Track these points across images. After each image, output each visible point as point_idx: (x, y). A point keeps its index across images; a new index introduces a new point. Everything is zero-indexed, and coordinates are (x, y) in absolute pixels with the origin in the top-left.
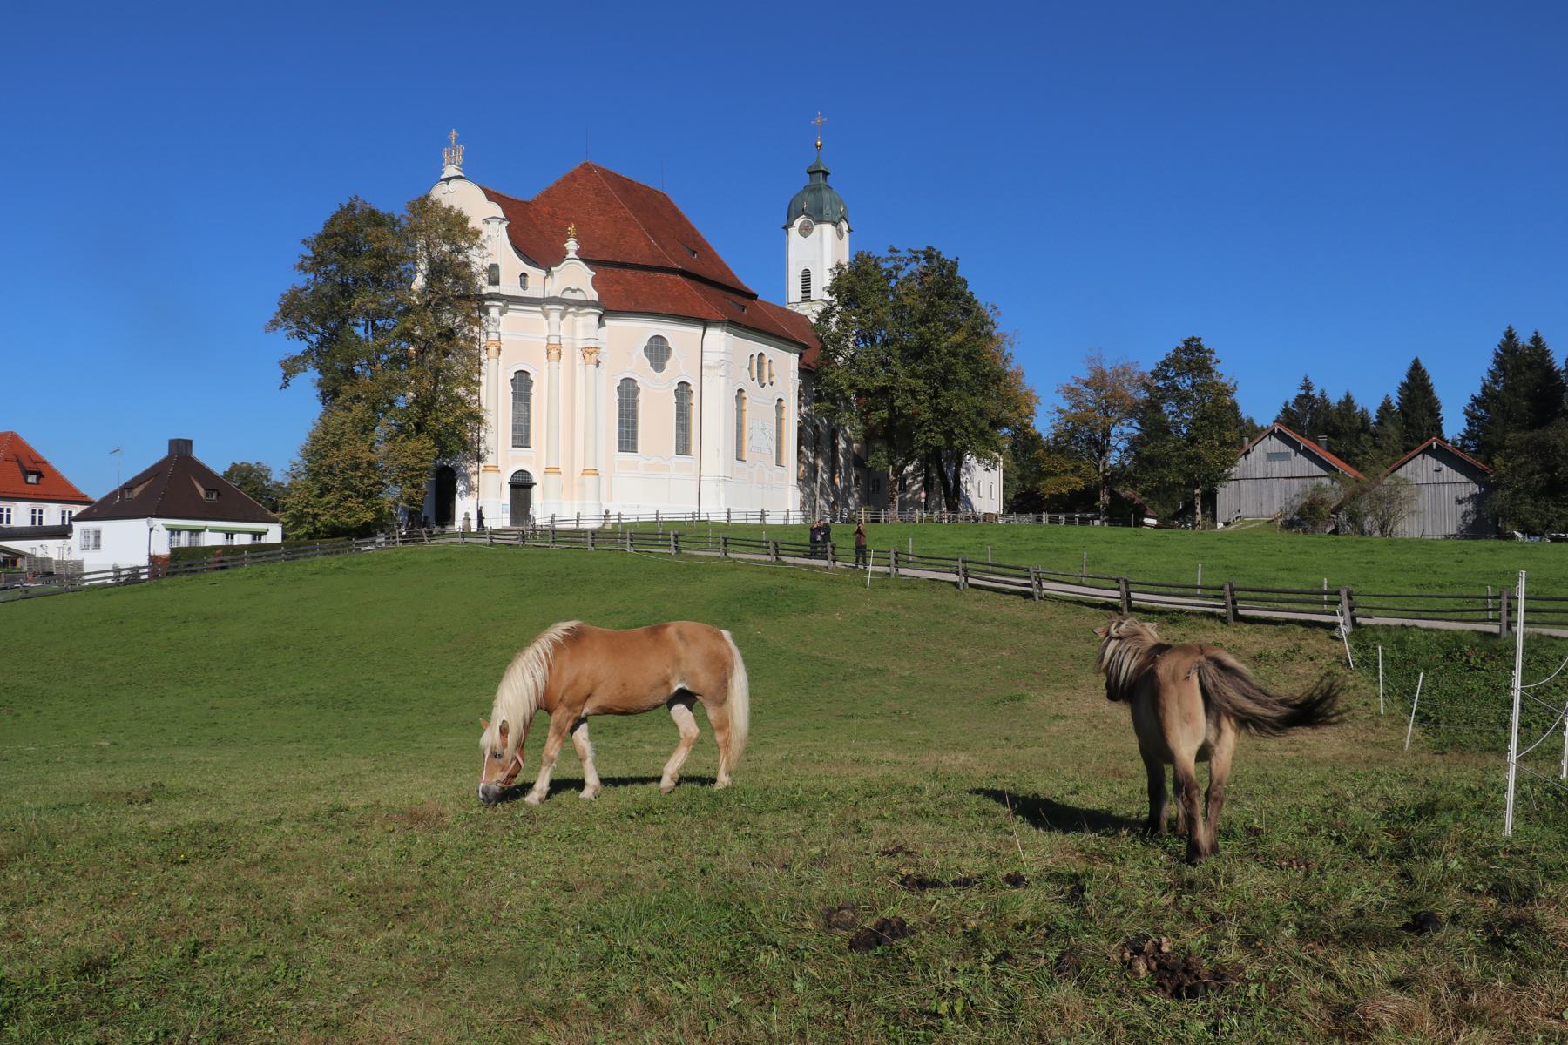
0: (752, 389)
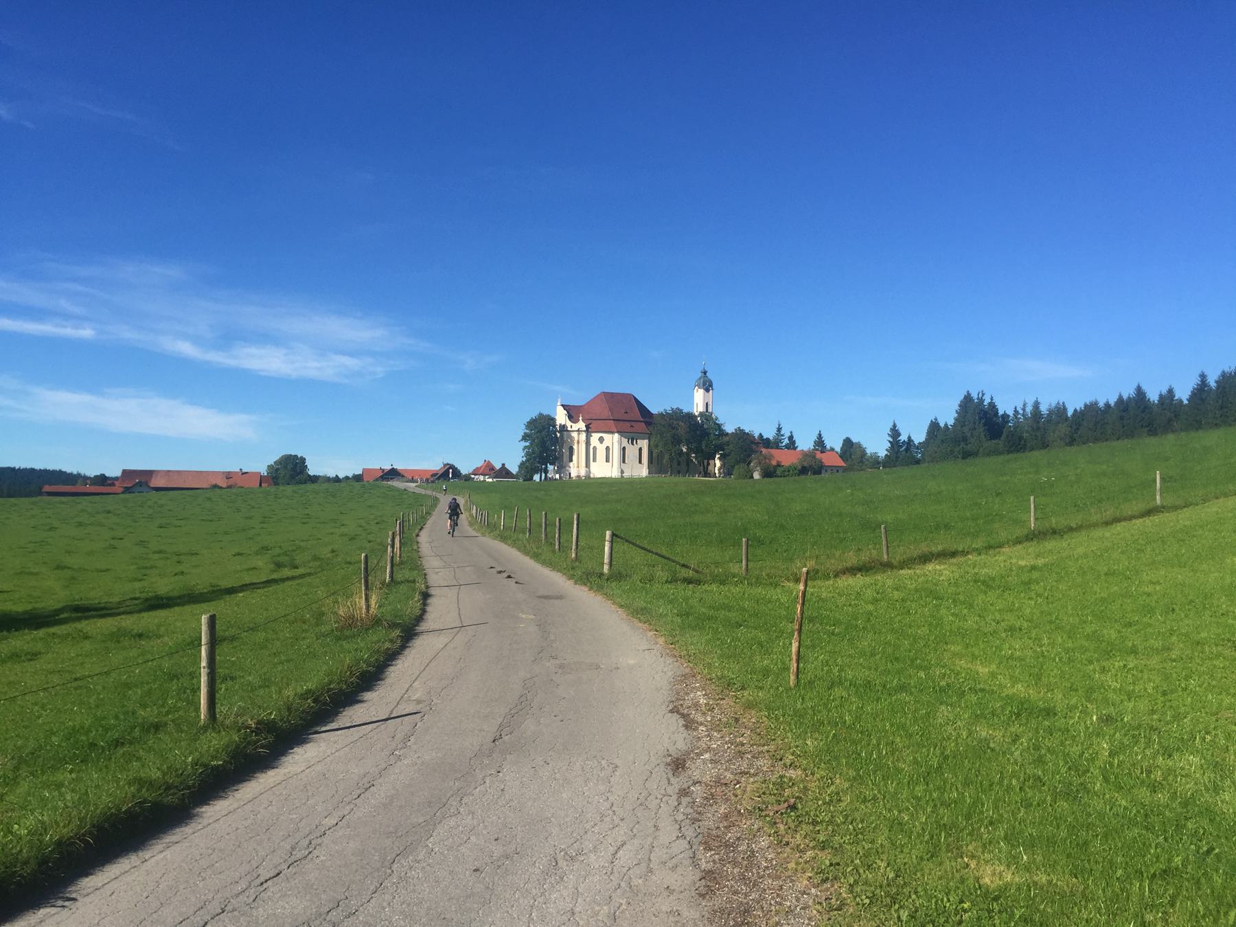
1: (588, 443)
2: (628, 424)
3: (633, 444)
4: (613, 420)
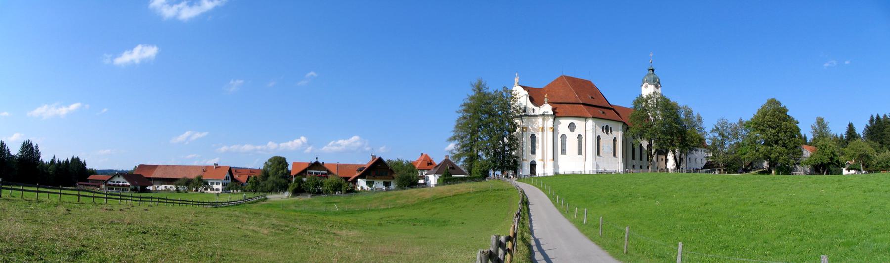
0: (603, 136)
1: (554, 130)
3: (607, 133)
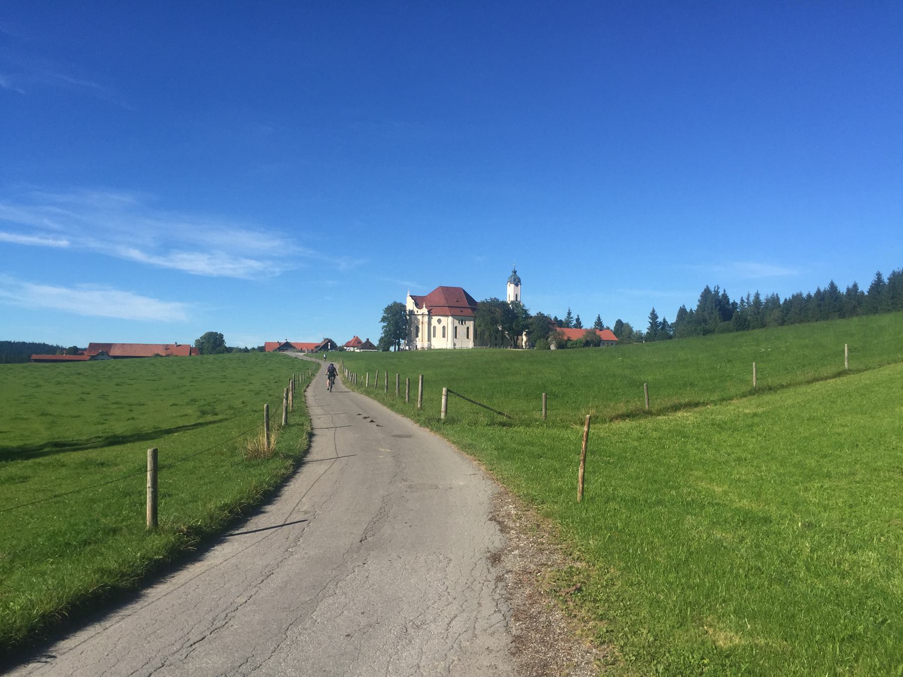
1: (429, 324)
2: (459, 310)
3: (462, 324)
4: (448, 306)
